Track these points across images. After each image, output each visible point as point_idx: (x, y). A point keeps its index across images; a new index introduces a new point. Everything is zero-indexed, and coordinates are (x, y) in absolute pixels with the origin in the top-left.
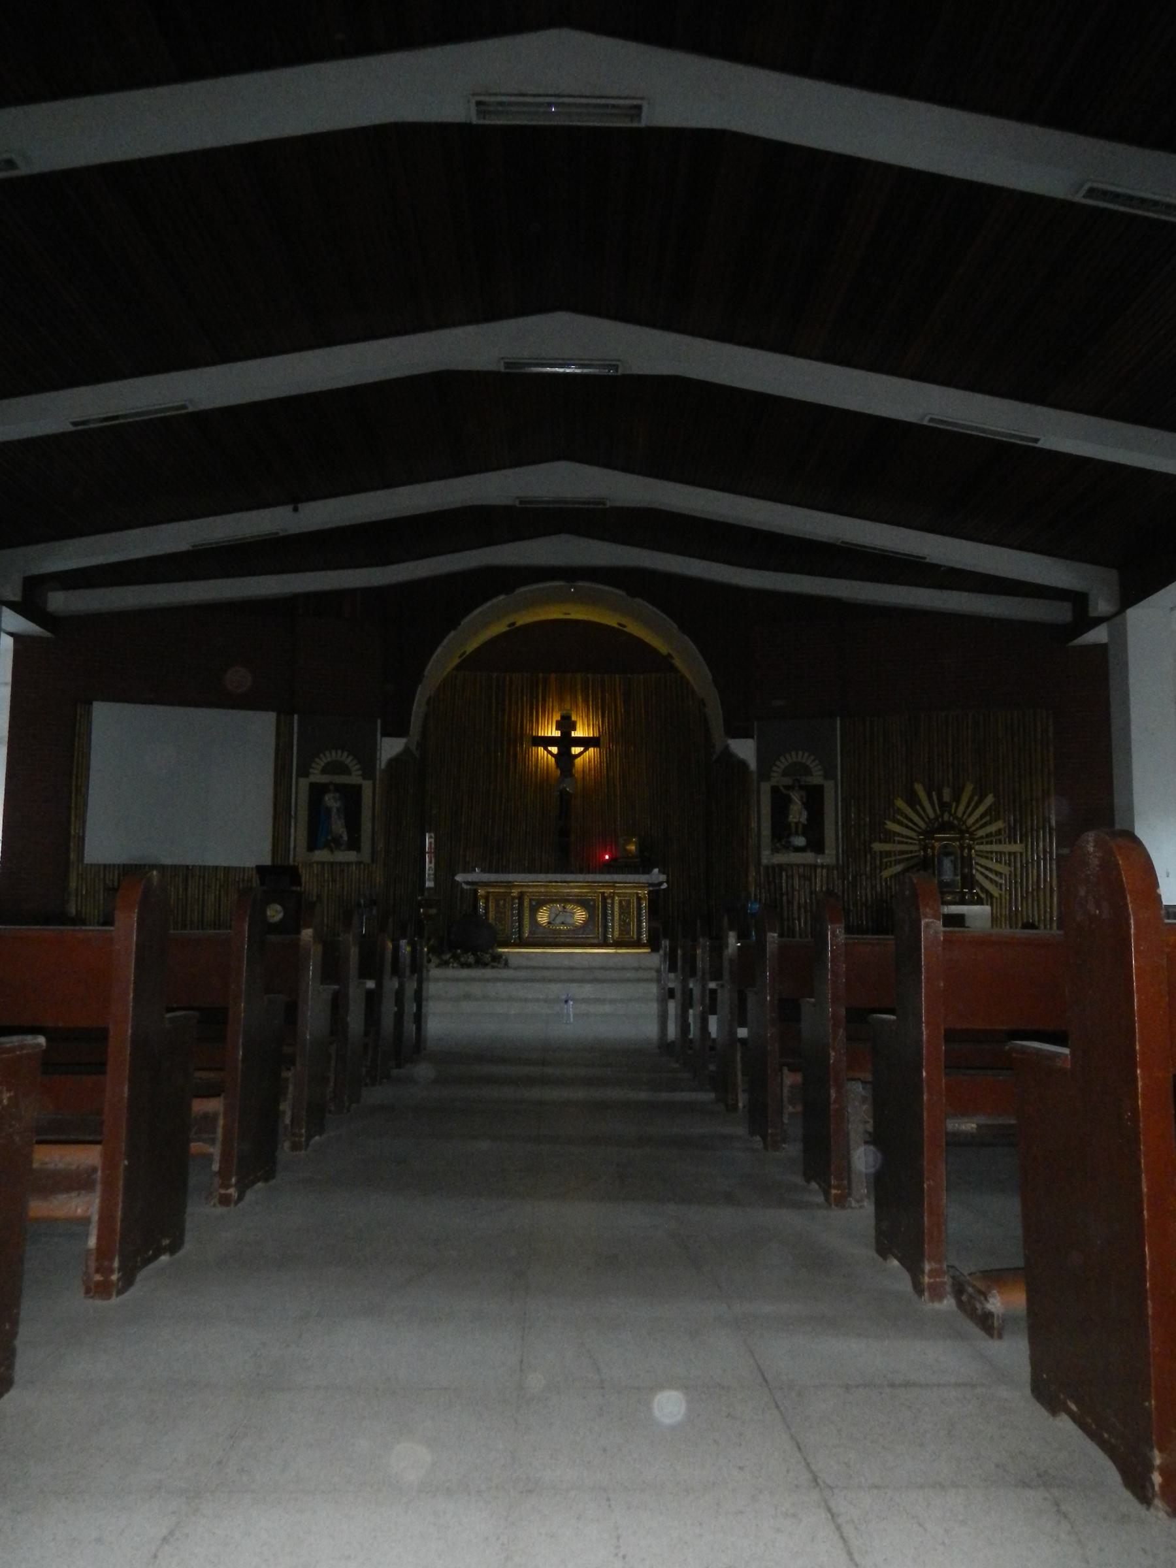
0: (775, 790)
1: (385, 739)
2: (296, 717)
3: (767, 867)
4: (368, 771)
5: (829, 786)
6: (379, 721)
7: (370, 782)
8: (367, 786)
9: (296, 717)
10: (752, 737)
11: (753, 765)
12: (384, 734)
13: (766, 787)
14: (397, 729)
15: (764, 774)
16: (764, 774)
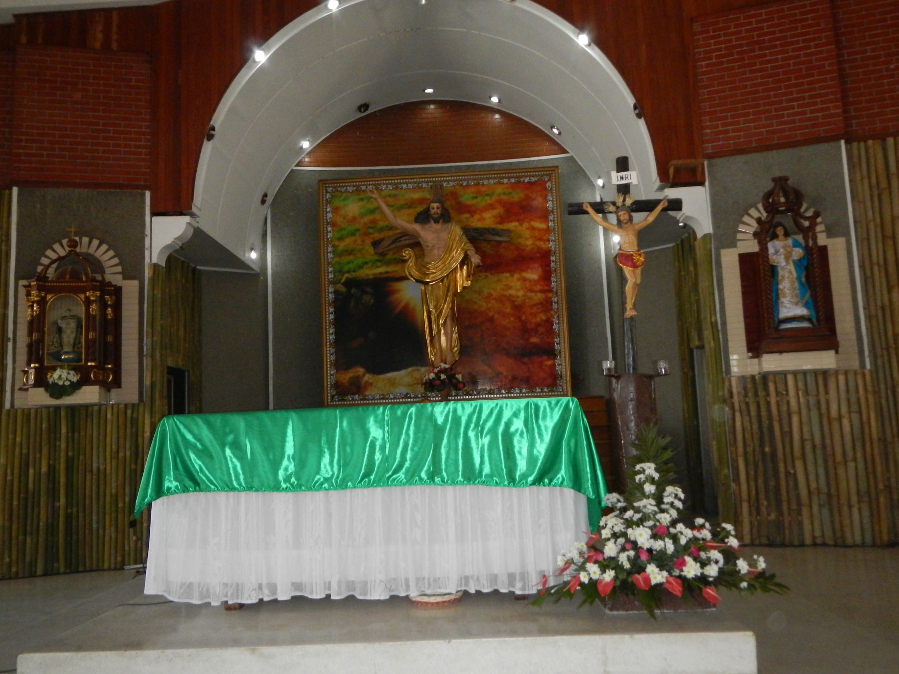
0: (746, 260)
1: (156, 219)
2: (15, 190)
3: (742, 379)
4: (132, 269)
5: (836, 248)
6: (148, 194)
7: (136, 283)
8: (130, 288)
9: (15, 190)
10: (702, 184)
11: (704, 225)
12: (154, 213)
13: (730, 260)
14: (176, 202)
15: (725, 234)
16: (725, 234)
